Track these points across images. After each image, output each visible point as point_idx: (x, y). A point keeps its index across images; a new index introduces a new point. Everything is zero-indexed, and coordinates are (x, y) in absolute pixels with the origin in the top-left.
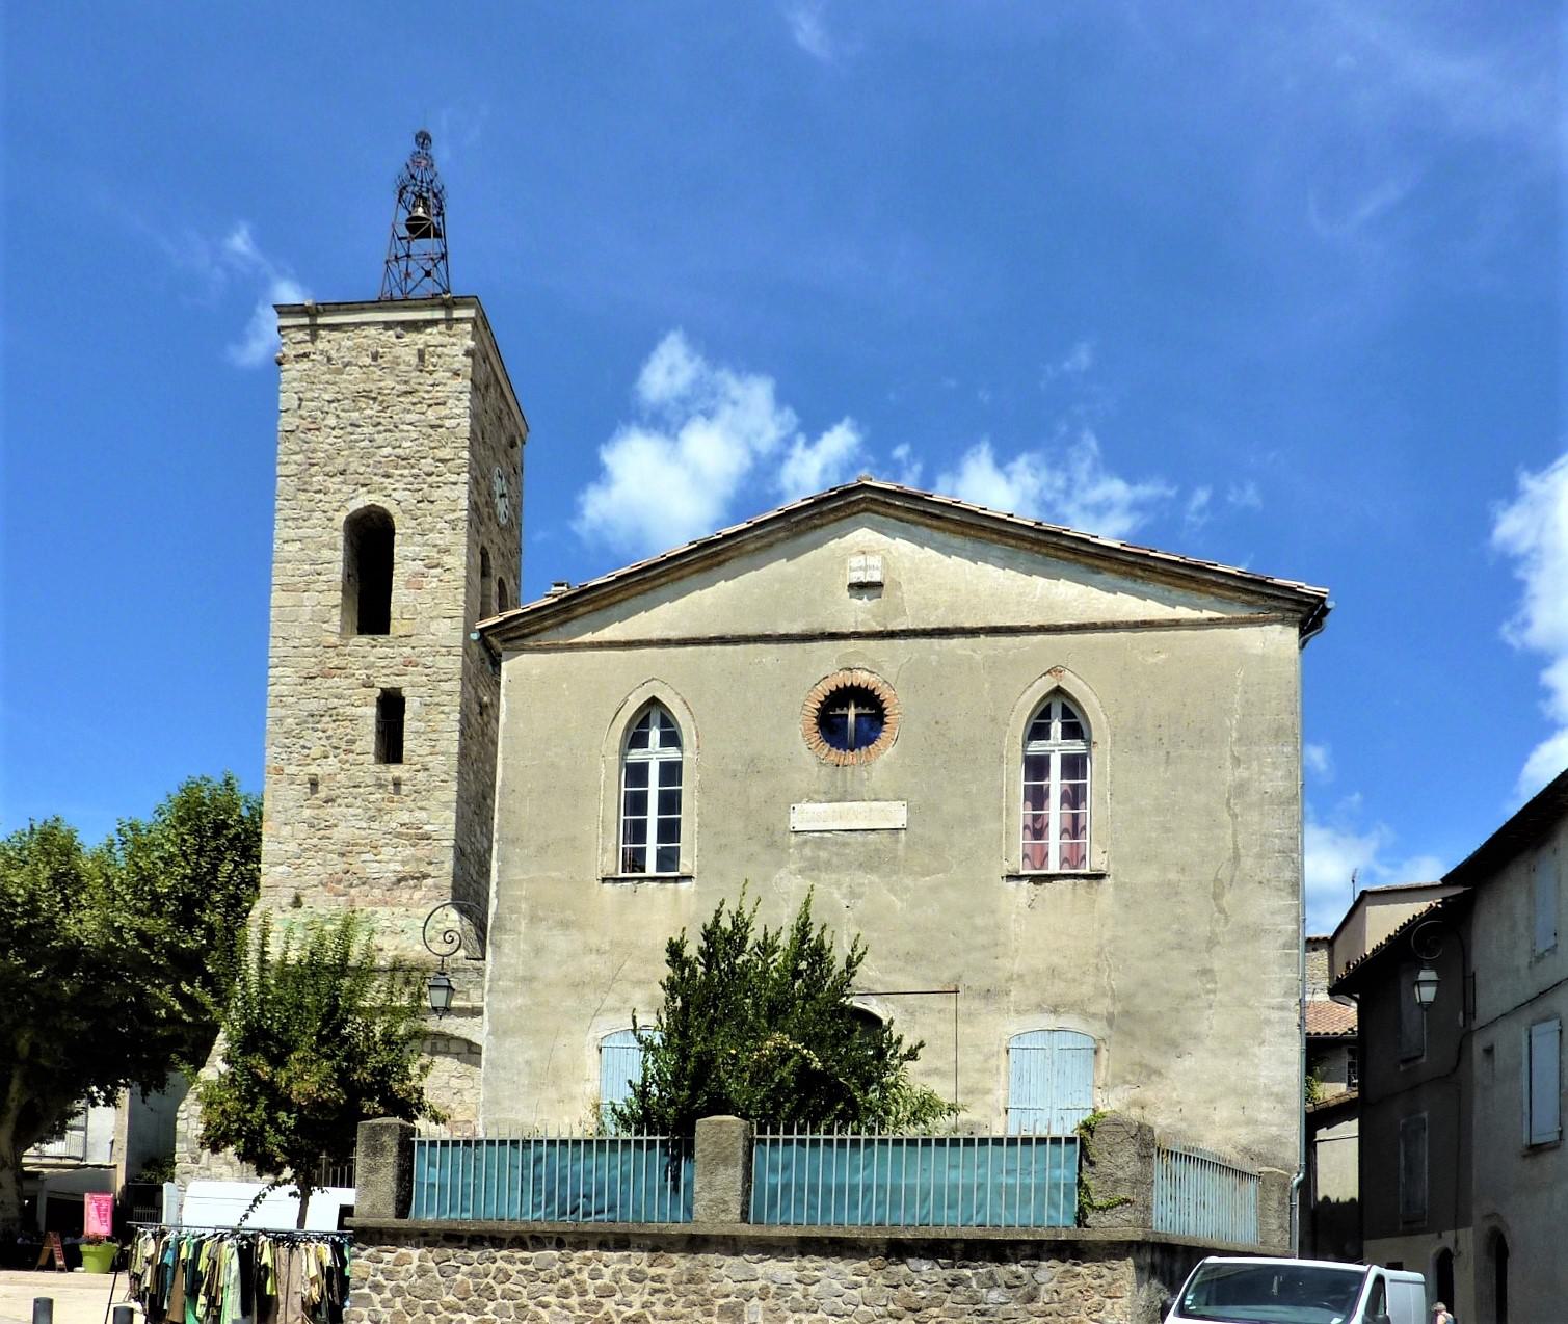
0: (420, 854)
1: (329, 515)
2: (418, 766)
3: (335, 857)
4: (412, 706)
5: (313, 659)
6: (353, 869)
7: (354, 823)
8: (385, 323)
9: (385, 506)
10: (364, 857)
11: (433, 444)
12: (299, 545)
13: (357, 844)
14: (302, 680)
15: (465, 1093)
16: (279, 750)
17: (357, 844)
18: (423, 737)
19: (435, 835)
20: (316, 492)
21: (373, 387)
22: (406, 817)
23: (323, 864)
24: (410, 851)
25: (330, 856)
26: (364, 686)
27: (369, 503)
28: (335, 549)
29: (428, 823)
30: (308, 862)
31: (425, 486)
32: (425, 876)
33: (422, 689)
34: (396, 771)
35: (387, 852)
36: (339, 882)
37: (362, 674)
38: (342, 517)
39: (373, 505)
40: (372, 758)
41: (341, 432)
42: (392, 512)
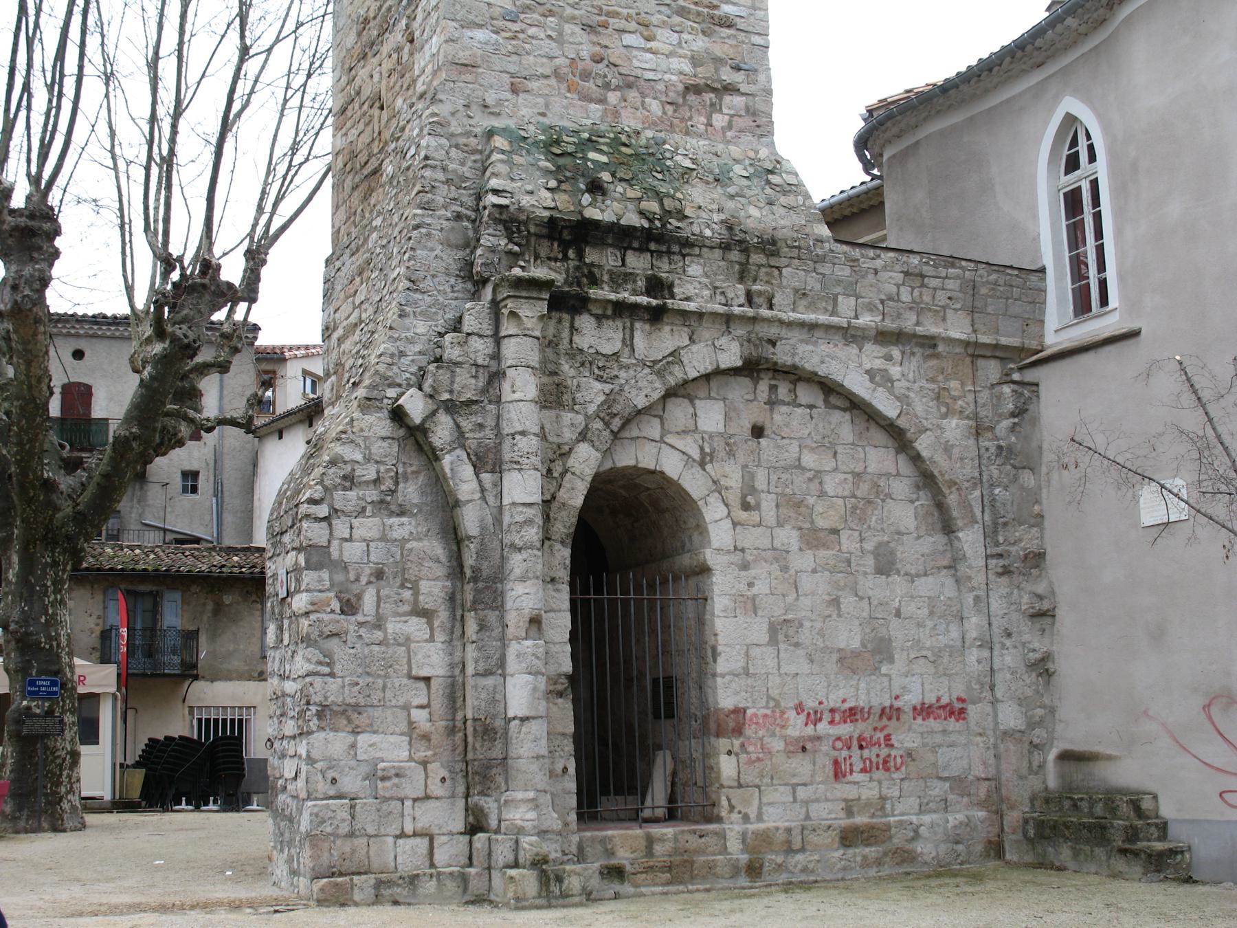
0: (718, 50)
3: (577, 29)
6: (615, 54)
10: (629, 39)
13: (616, 15)
15: (827, 478)
17: (616, 15)
19: (741, 24)
23: (559, 39)
24: (699, 44)
25: (568, 28)
30: (532, 31)
32: (730, 89)
35: (665, 39)
36: (586, 75)
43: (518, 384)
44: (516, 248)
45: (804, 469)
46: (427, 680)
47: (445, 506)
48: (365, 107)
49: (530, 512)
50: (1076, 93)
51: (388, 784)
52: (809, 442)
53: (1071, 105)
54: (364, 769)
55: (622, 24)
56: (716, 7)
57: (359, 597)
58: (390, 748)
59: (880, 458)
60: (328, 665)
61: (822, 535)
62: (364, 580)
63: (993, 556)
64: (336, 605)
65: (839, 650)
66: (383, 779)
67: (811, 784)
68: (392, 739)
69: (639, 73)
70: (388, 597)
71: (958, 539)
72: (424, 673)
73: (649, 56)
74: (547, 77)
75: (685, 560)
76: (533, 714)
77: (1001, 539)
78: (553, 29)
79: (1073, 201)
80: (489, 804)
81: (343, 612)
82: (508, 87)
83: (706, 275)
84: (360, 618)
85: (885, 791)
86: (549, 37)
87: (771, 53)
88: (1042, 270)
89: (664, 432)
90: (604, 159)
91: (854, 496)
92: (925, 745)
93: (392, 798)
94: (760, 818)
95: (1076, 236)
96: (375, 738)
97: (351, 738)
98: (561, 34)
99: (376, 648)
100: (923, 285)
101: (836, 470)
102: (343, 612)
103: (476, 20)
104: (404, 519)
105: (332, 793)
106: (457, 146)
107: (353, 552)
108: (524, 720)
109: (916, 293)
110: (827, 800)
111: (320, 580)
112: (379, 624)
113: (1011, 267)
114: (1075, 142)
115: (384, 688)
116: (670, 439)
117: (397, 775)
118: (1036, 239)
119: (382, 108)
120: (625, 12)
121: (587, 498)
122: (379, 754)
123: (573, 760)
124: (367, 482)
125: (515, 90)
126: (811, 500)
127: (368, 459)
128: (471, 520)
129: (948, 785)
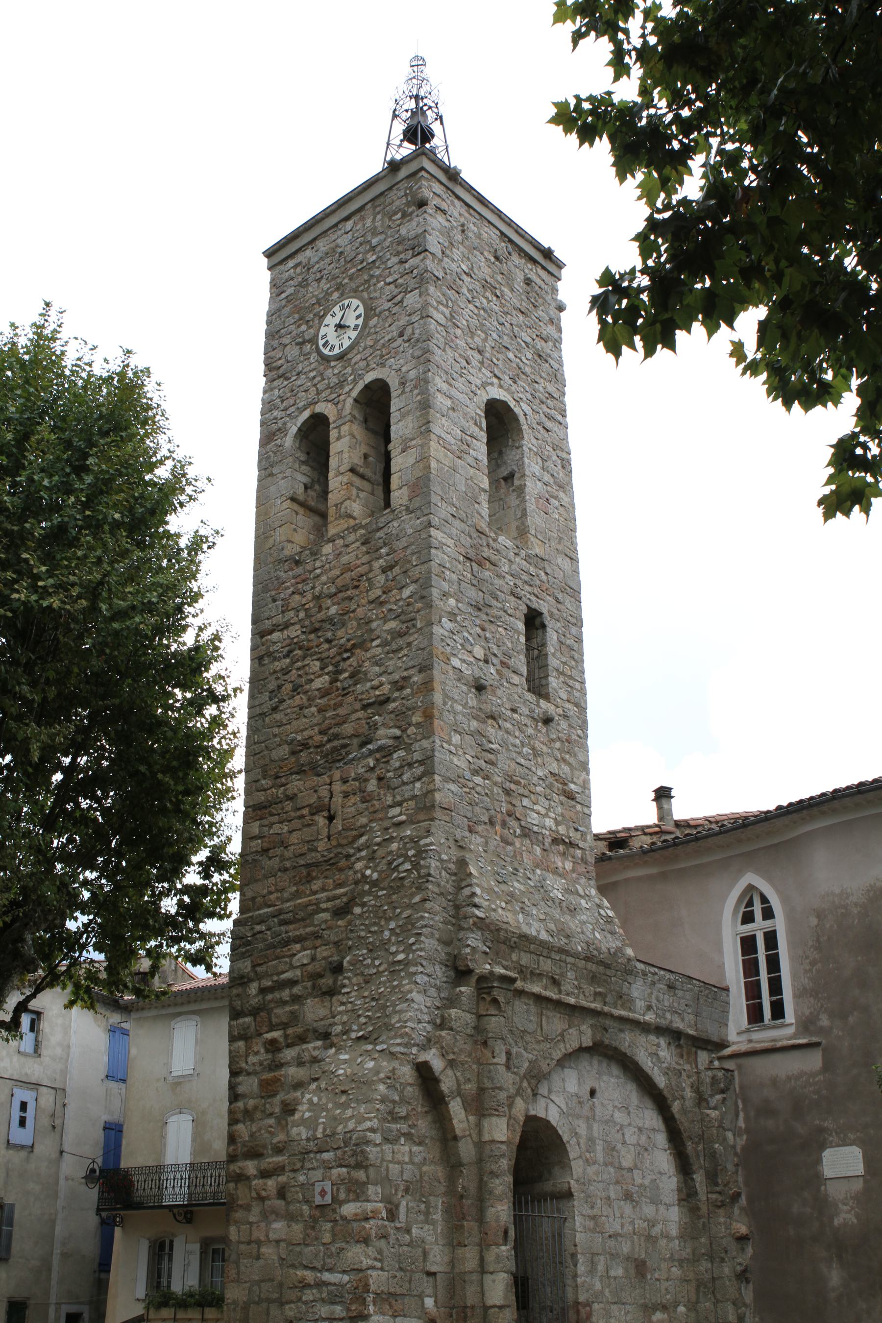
1: (474, 388)
8: (502, 233)
9: (517, 410)
10: (526, 802)
12: (449, 403)
13: (517, 783)
15: (626, 1130)
16: (446, 634)
18: (562, 679)
22: (554, 767)
33: (558, 624)
41: (476, 311)
43: (497, 1051)
45: (615, 1124)
46: (434, 1274)
47: (447, 1137)
48: (305, 811)
49: (504, 1147)
50: (757, 872)
52: (616, 1103)
53: (751, 878)
55: (522, 791)
57: (397, 1206)
59: (651, 1119)
60: (380, 1261)
61: (624, 1172)
62: (400, 1194)
63: (712, 1193)
64: (384, 1214)
69: (531, 827)
71: (693, 1180)
72: (433, 1269)
73: (535, 815)
75: (547, 1187)
77: (720, 1181)
79: (748, 944)
83: (576, 979)
84: (398, 1225)
87: (592, 818)
88: (727, 990)
89: (550, 1091)
90: (522, 888)
91: (639, 1145)
95: (750, 968)
99: (405, 1248)
101: (629, 1125)
103: (452, 777)
104: (421, 1148)
108: (501, 1307)
112: (408, 1231)
114: (750, 903)
115: (410, 1283)
116: (553, 1097)
118: (722, 966)
119: (331, 818)
121: (521, 1137)
124: (401, 1118)
125: (470, 831)
126: (619, 1146)
128: (466, 1150)
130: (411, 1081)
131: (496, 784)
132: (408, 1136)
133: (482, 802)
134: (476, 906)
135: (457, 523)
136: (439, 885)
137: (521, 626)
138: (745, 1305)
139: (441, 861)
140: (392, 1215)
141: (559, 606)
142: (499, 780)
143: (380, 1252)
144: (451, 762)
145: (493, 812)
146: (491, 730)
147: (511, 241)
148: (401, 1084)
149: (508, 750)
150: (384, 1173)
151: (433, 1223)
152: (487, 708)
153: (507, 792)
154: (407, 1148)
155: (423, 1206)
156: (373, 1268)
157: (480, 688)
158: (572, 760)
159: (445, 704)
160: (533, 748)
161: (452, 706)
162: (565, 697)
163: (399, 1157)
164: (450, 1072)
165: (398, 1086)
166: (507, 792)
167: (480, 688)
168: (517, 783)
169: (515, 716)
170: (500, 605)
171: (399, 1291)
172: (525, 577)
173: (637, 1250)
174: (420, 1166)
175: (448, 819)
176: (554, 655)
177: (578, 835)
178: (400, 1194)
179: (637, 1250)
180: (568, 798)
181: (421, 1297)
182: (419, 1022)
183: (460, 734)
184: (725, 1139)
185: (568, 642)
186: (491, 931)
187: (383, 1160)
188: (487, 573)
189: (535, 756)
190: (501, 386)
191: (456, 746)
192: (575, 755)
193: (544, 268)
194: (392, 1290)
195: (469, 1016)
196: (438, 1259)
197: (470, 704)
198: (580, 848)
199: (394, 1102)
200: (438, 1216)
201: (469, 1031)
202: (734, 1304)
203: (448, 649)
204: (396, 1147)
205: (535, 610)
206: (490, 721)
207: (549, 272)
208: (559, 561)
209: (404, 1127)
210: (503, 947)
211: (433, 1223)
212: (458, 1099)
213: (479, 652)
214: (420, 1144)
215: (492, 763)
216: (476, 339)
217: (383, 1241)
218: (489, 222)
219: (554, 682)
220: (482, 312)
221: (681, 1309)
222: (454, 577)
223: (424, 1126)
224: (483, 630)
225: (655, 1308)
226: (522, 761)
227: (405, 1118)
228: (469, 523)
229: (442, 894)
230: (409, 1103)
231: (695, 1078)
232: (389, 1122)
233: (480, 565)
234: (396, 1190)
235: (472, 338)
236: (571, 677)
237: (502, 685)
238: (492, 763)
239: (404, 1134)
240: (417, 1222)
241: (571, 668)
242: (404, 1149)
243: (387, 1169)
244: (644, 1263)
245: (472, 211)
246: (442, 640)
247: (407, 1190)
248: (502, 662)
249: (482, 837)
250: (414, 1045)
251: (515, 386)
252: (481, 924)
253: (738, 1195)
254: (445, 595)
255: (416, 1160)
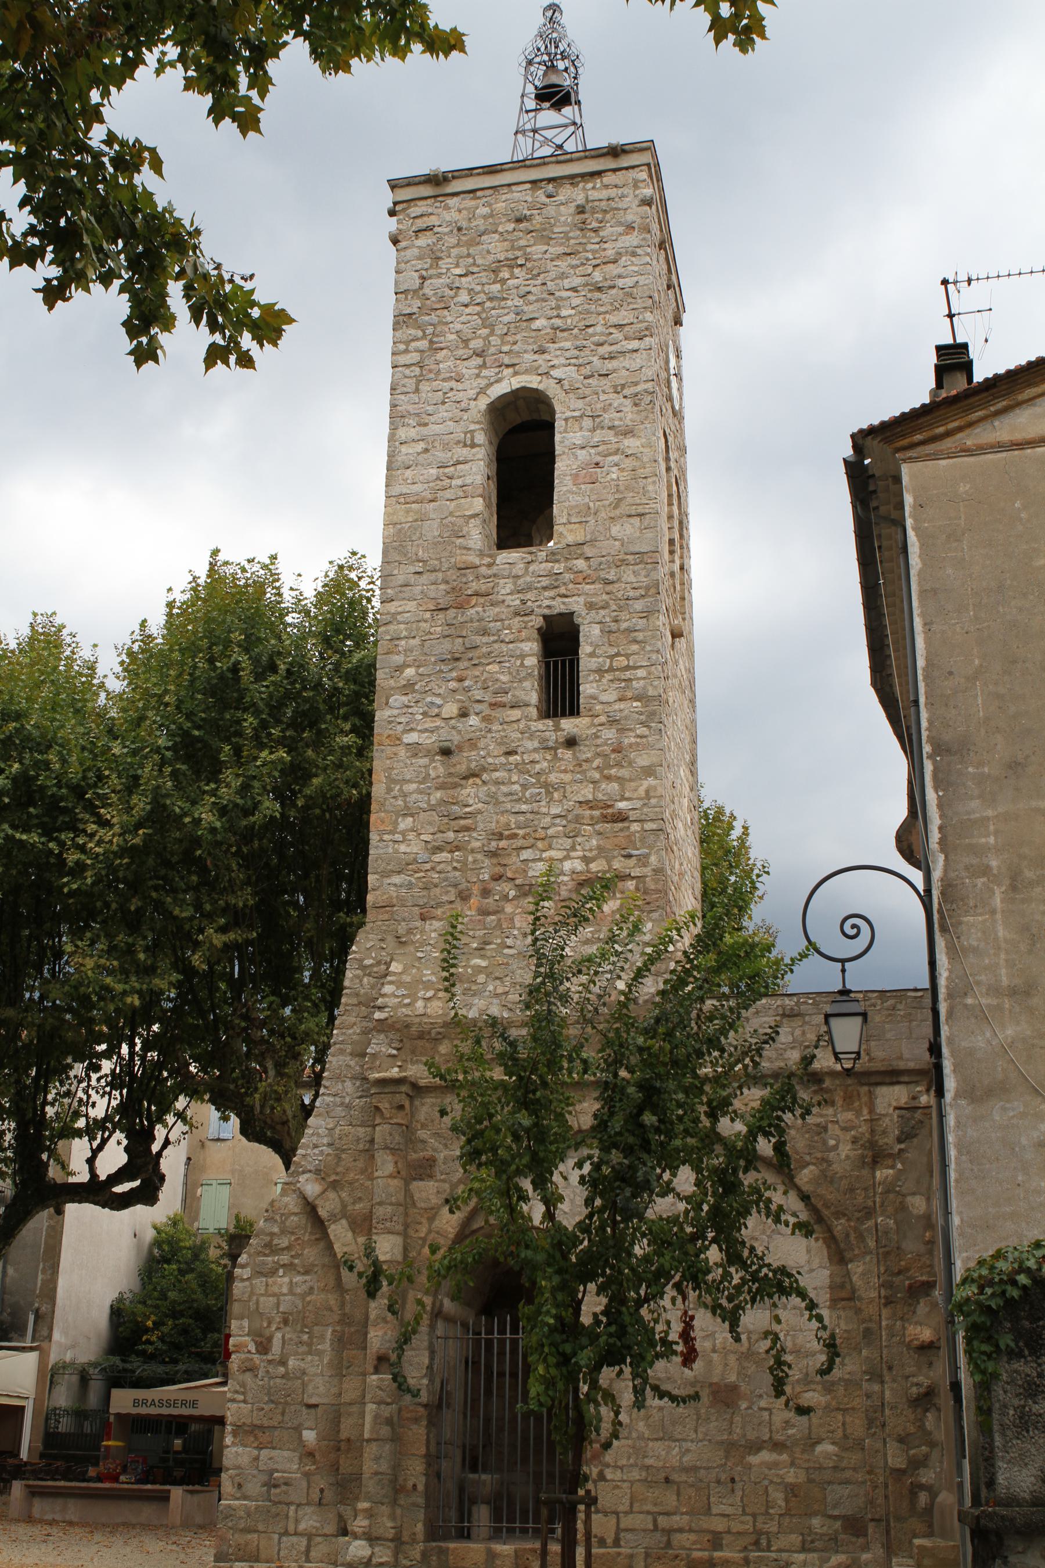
1: (463, 405)
2: (603, 719)
4: (590, 634)
5: (443, 587)
7: (509, 806)
8: (533, 182)
9: (541, 387)
10: (525, 855)
11: (602, 309)
12: (422, 445)
14: (428, 615)
18: (608, 677)
20: (444, 380)
21: (519, 253)
22: (587, 793)
26: (517, 614)
27: (518, 386)
28: (473, 445)
29: (623, 799)
31: (595, 359)
34: (569, 725)
37: (515, 601)
38: (483, 403)
39: (524, 388)
40: (533, 712)
41: (478, 308)
42: (550, 393)
44: (394, 1052)
46: (316, 1406)
51: (278, 1491)
54: (264, 1478)
55: (520, 843)
56: (609, 806)
57: (270, 1339)
58: (285, 1461)
60: (243, 1393)
62: (274, 1327)
64: (252, 1347)
65: (711, 1384)
66: (276, 1486)
67: (675, 1514)
68: (286, 1454)
70: (291, 1339)
72: (313, 1401)
74: (451, 902)
76: (375, 1436)
78: (458, 861)
80: (347, 1511)
81: (258, 1352)
82: (417, 917)
84: (270, 1357)
85: (759, 1525)
86: (455, 868)
92: (810, 1481)
93: (280, 1503)
94: (617, 1543)
96: (275, 1453)
97: (256, 1452)
98: (465, 863)
99: (278, 1380)
100: (805, 1023)
102: (258, 1352)
105: (238, 1495)
106: (369, 975)
107: (267, 1303)
108: (368, 1441)
109: (798, 1032)
110: (691, 1530)
111: (241, 1328)
112: (283, 1363)
113: (916, 990)
115: (283, 1414)
117: (286, 1484)
120: (521, 832)
122: (276, 1466)
123: (423, 1479)
124: (283, 1249)
127: (283, 1232)
129: (838, 1524)
130: (296, 1210)
131: (472, 851)
132: (289, 1267)
133: (446, 879)
134: (380, 1008)
135: (425, 579)
136: (357, 995)
137: (532, 647)
138: (932, 1445)
139: (363, 968)
140: (264, 1347)
141: (609, 588)
142: (476, 844)
143: (243, 1385)
144: (396, 851)
145: (463, 886)
146: (469, 792)
147: (550, 180)
148: (282, 1215)
149: (498, 803)
150: (253, 1307)
151: (320, 1353)
152: (462, 768)
153: (493, 854)
154: (286, 1280)
155: (305, 1337)
156: (233, 1400)
157: (446, 752)
158: (624, 773)
159: (389, 790)
160: (546, 785)
161: (401, 790)
162: (610, 696)
163: (276, 1289)
164: (331, 1195)
165: (278, 1217)
166: (493, 854)
167: (446, 752)
168: (514, 836)
169: (511, 759)
170: (492, 638)
171: (266, 1423)
172: (545, 581)
173: (718, 1370)
174: (303, 1296)
175: (386, 917)
176: (592, 655)
177: (632, 862)
178: (274, 1327)
179: (718, 1370)
180: (614, 822)
181: (298, 1429)
182: (316, 1146)
183: (412, 815)
184: (903, 1208)
185: (624, 625)
186: (398, 1030)
187: (252, 1293)
188: (472, 611)
189: (548, 792)
190: (516, 374)
191: (403, 833)
192: (630, 764)
193: (615, 170)
194: (258, 1422)
195: (361, 1130)
196: (322, 1389)
197: (433, 774)
198: (633, 878)
199: (272, 1234)
200: (326, 1346)
201: (361, 1146)
202: (901, 1440)
203: (400, 728)
204: (270, 1280)
205: (561, 614)
206: (471, 781)
207: (627, 168)
208: (615, 530)
209: (285, 1258)
210: (420, 1043)
211: (320, 1353)
212: (344, 1222)
213: (451, 709)
214: (306, 1273)
215: (467, 829)
216: (473, 344)
217: (248, 1374)
218: (509, 185)
219: (587, 688)
220: (488, 304)
221: (827, 1448)
222: (416, 642)
223: (312, 1254)
224: (461, 680)
225: (756, 1447)
226: (524, 807)
227: (288, 1248)
228: (445, 566)
229: (360, 1003)
230: (293, 1233)
231: (864, 1129)
232: (265, 1255)
233: (460, 607)
234: (269, 1324)
235: (467, 346)
236: (628, 668)
237: (490, 731)
238: (467, 829)
239: (284, 1265)
240: (296, 1353)
241: (627, 656)
242: (282, 1281)
243: (257, 1303)
244: (733, 1388)
245: (479, 194)
246: (390, 722)
247: (286, 1322)
248: (491, 705)
249: (441, 920)
250: (304, 1172)
251: (546, 356)
252: (383, 1026)
253: (930, 1286)
254: (400, 669)
255: (299, 1290)
